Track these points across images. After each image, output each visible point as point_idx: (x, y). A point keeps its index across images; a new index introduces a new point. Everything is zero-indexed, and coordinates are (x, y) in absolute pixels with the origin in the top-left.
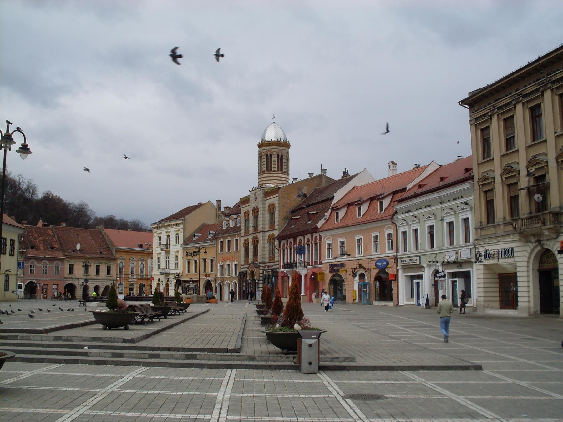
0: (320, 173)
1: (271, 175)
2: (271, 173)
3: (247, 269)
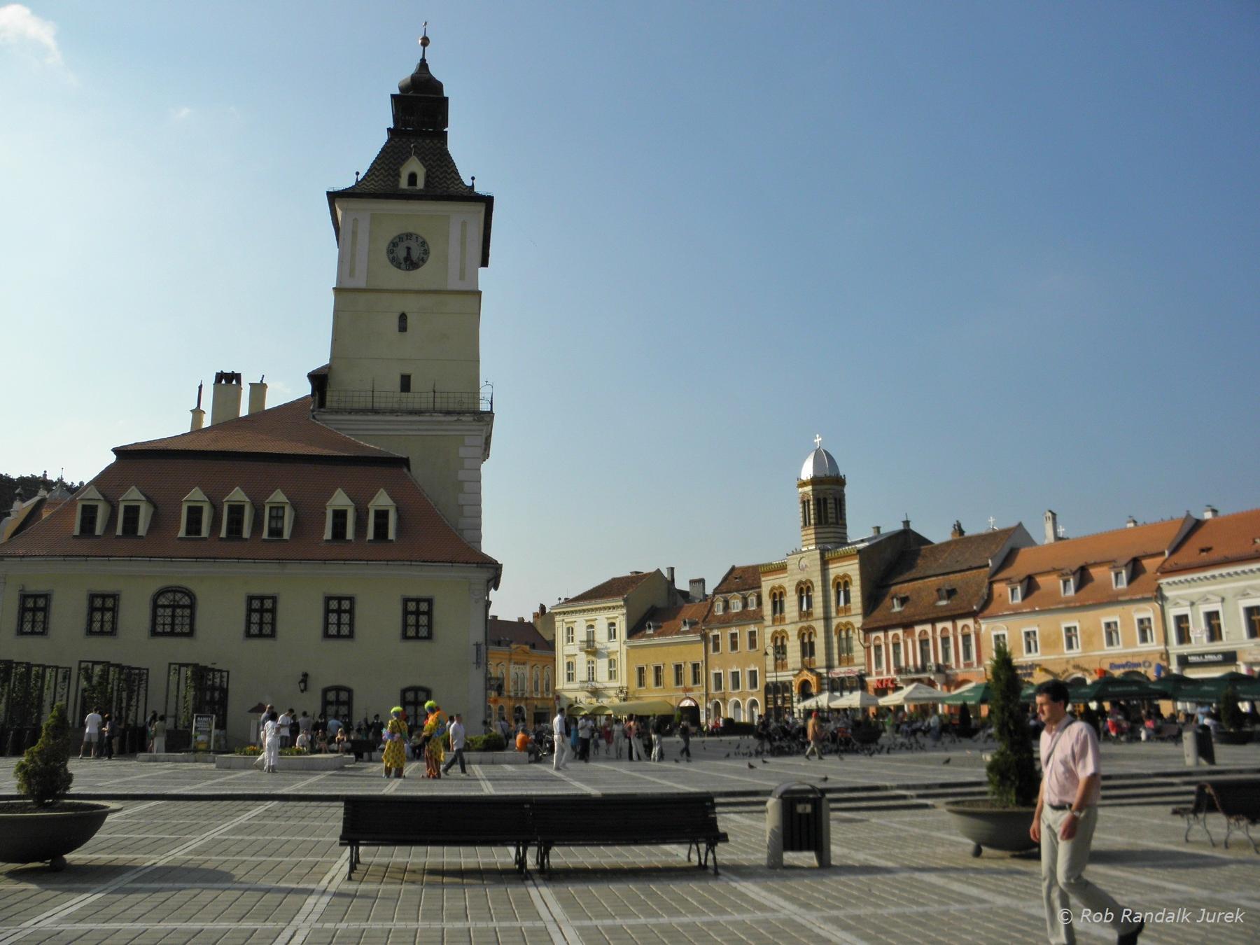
0: (900, 527)
3: (792, 678)
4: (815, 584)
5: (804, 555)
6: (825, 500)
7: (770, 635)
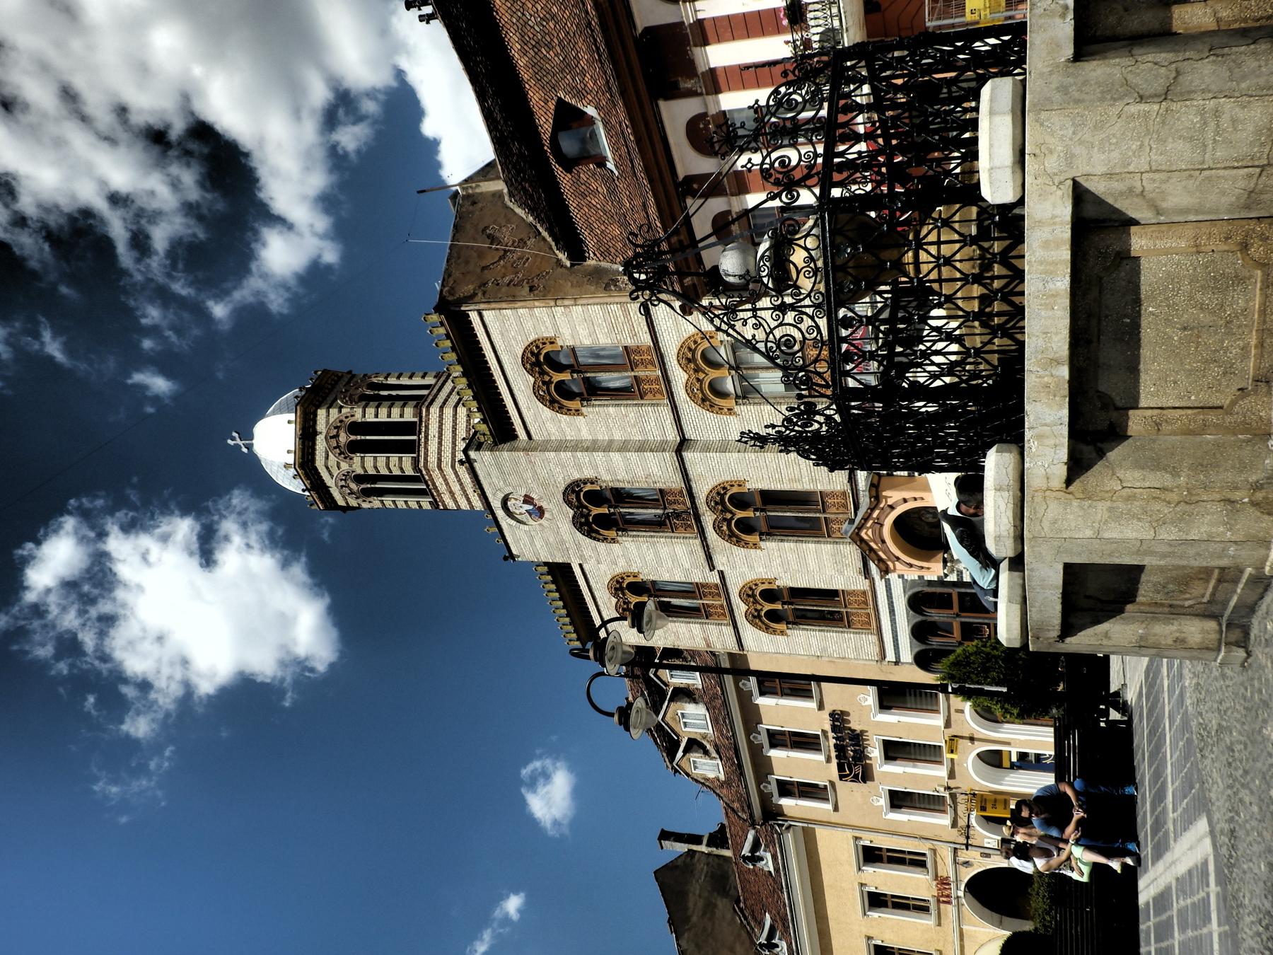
1: (433, 430)
2: (427, 427)
6: (355, 428)
7: (763, 636)
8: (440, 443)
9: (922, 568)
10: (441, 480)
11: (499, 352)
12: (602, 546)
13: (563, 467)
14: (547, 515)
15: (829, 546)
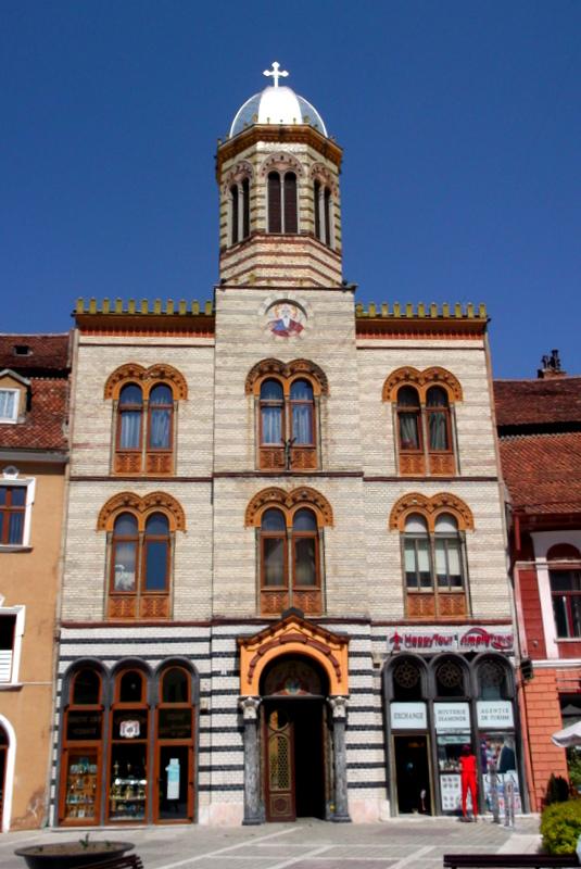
2: (331, 256)
4: (331, 378)
5: (291, 295)
8: (322, 263)
9: (250, 676)
10: (294, 251)
11: (446, 352)
12: (242, 376)
13: (341, 370)
14: (279, 338)
15: (253, 591)
